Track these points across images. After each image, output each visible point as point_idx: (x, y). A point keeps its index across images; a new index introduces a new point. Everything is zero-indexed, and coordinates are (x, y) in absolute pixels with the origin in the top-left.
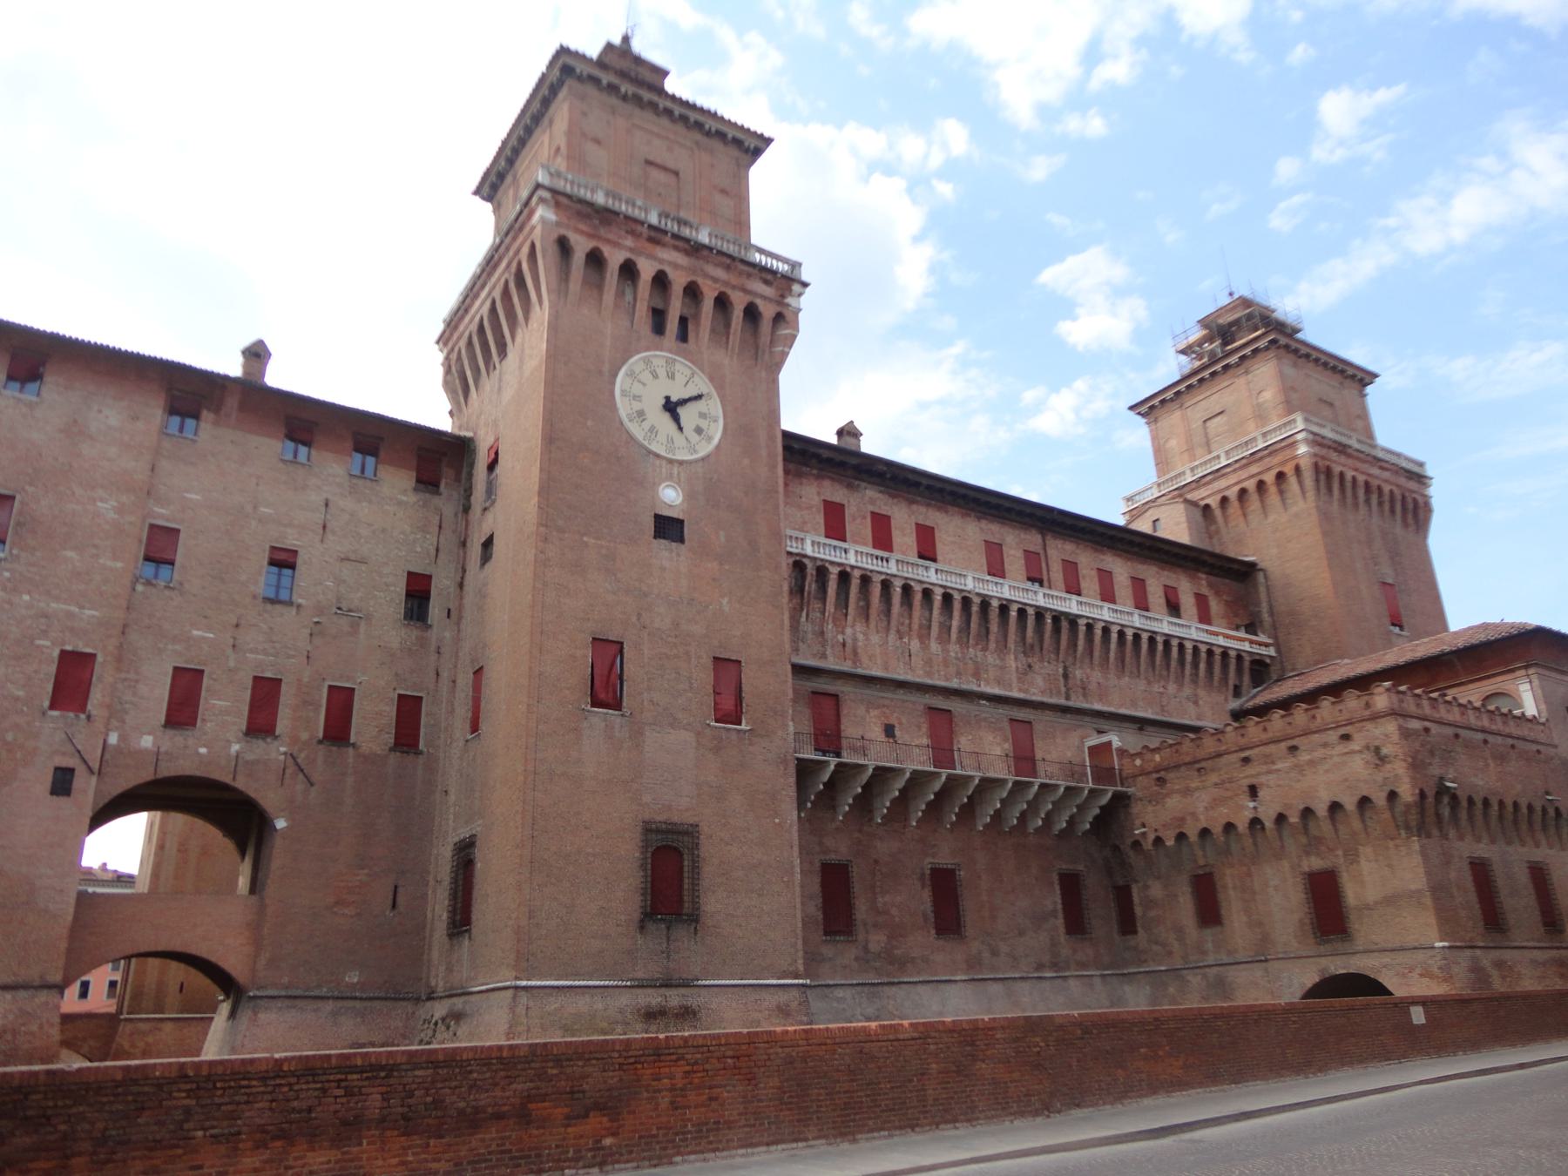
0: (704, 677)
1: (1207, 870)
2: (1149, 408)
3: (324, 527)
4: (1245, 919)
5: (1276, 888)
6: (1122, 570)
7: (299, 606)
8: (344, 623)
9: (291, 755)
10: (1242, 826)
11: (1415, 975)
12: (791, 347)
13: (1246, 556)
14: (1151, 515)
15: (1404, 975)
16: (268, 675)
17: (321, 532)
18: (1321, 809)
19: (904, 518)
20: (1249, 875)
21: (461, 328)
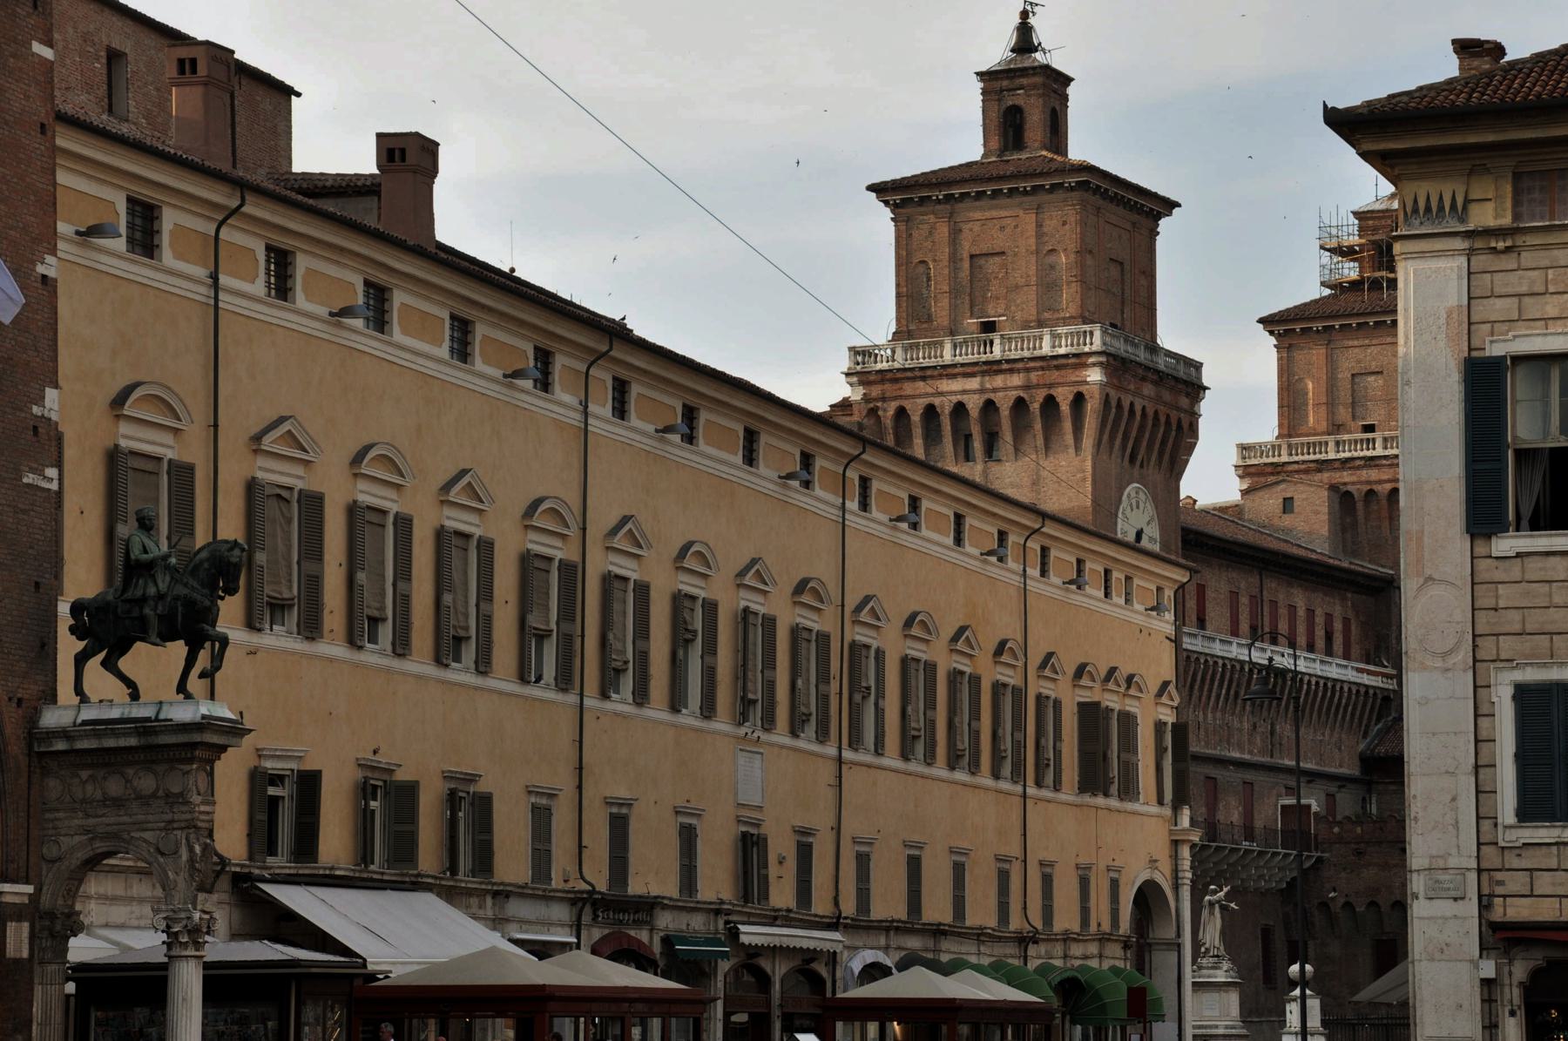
2: (1283, 326)
6: (1300, 599)
12: (1190, 454)
13: (1383, 566)
14: (1284, 490)
21: (908, 388)
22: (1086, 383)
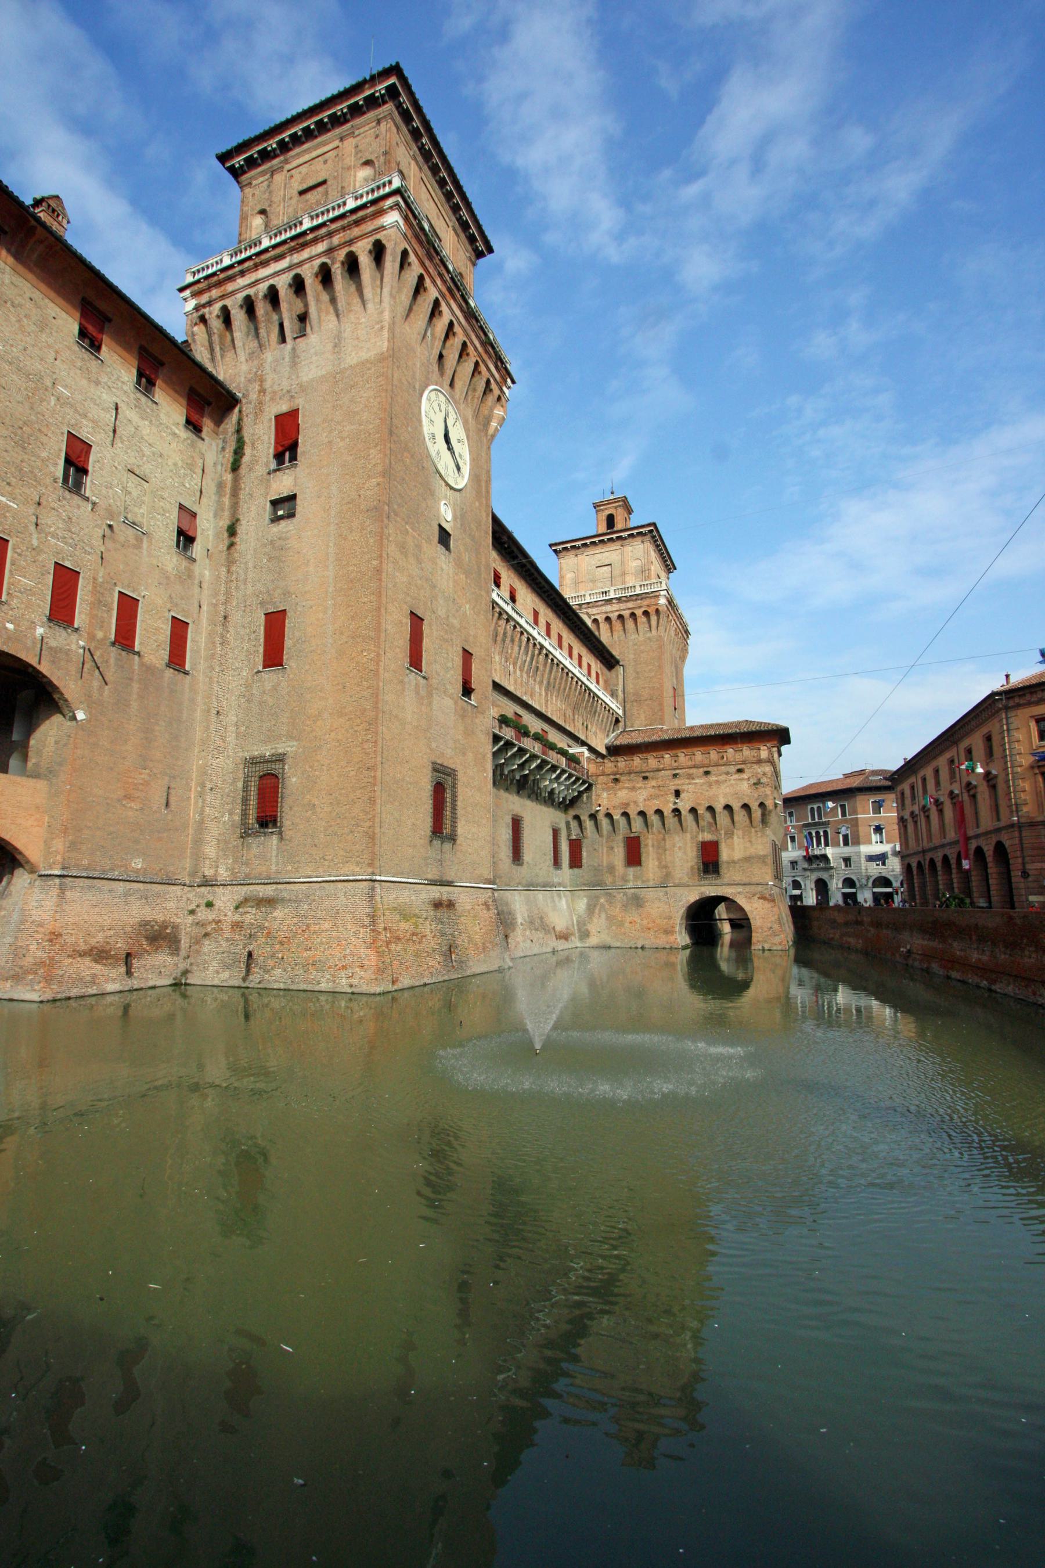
0: (458, 661)
1: (636, 835)
3: (115, 431)
4: (657, 863)
5: (680, 848)
7: (94, 504)
8: (130, 532)
9: (89, 650)
10: (667, 812)
11: (756, 898)
15: (750, 898)
16: (67, 564)
17: (112, 434)
18: (719, 808)
19: (508, 577)
20: (664, 839)
21: (230, 287)
22: (382, 228)
